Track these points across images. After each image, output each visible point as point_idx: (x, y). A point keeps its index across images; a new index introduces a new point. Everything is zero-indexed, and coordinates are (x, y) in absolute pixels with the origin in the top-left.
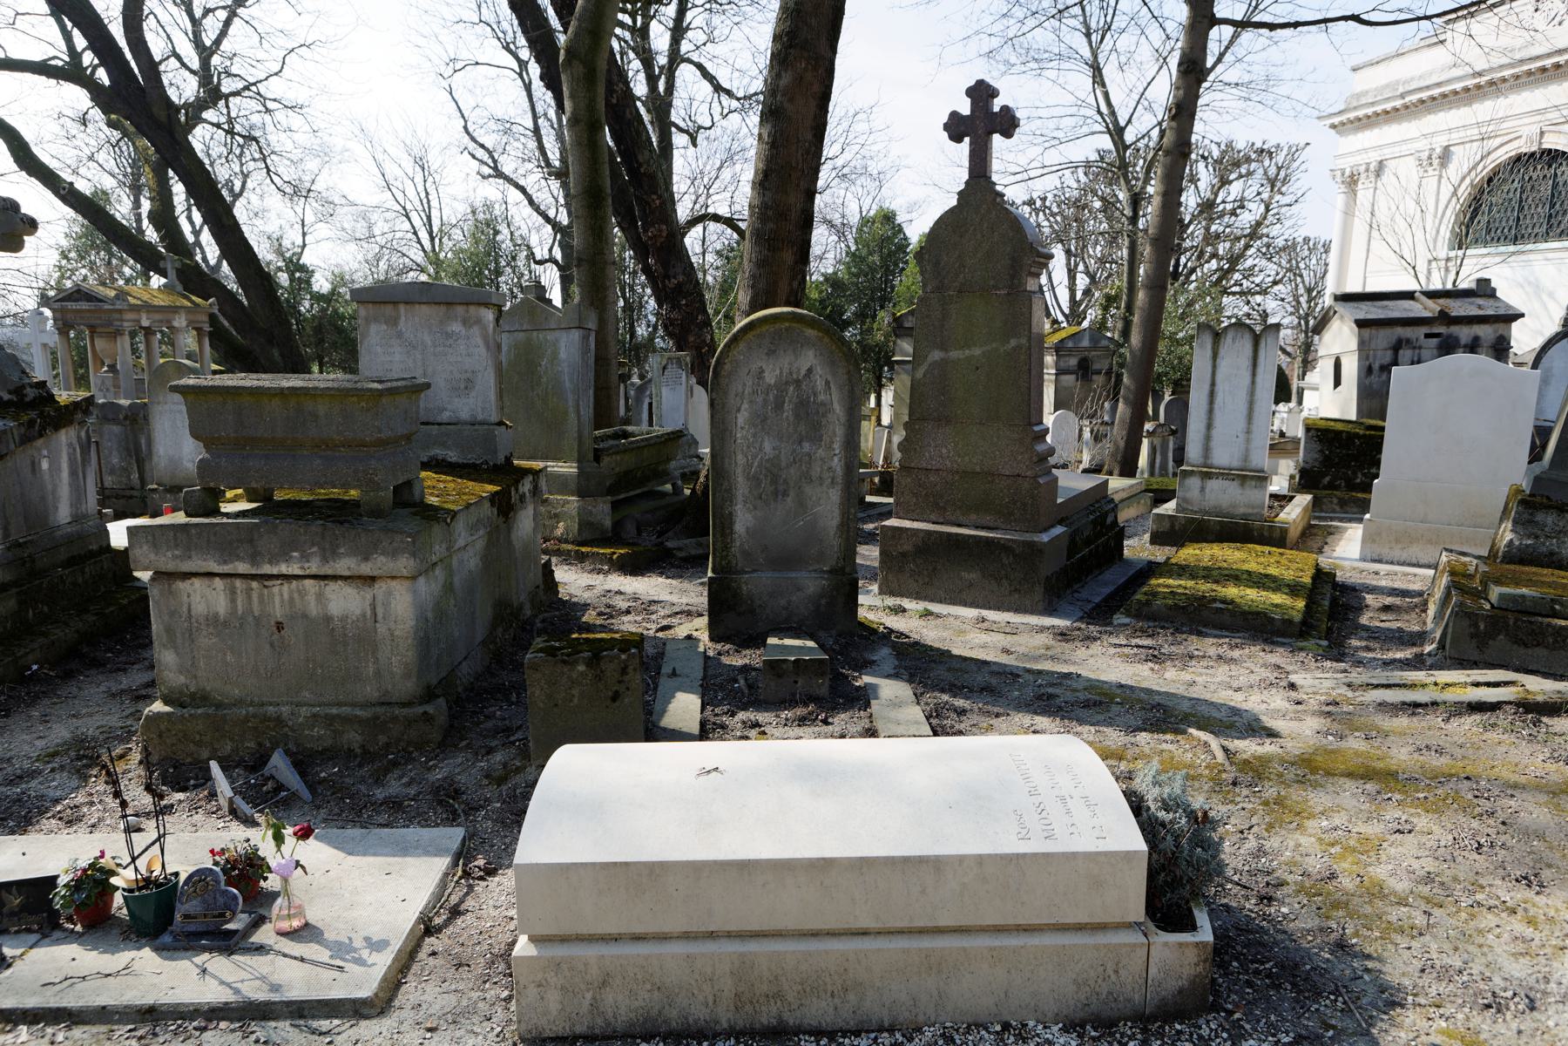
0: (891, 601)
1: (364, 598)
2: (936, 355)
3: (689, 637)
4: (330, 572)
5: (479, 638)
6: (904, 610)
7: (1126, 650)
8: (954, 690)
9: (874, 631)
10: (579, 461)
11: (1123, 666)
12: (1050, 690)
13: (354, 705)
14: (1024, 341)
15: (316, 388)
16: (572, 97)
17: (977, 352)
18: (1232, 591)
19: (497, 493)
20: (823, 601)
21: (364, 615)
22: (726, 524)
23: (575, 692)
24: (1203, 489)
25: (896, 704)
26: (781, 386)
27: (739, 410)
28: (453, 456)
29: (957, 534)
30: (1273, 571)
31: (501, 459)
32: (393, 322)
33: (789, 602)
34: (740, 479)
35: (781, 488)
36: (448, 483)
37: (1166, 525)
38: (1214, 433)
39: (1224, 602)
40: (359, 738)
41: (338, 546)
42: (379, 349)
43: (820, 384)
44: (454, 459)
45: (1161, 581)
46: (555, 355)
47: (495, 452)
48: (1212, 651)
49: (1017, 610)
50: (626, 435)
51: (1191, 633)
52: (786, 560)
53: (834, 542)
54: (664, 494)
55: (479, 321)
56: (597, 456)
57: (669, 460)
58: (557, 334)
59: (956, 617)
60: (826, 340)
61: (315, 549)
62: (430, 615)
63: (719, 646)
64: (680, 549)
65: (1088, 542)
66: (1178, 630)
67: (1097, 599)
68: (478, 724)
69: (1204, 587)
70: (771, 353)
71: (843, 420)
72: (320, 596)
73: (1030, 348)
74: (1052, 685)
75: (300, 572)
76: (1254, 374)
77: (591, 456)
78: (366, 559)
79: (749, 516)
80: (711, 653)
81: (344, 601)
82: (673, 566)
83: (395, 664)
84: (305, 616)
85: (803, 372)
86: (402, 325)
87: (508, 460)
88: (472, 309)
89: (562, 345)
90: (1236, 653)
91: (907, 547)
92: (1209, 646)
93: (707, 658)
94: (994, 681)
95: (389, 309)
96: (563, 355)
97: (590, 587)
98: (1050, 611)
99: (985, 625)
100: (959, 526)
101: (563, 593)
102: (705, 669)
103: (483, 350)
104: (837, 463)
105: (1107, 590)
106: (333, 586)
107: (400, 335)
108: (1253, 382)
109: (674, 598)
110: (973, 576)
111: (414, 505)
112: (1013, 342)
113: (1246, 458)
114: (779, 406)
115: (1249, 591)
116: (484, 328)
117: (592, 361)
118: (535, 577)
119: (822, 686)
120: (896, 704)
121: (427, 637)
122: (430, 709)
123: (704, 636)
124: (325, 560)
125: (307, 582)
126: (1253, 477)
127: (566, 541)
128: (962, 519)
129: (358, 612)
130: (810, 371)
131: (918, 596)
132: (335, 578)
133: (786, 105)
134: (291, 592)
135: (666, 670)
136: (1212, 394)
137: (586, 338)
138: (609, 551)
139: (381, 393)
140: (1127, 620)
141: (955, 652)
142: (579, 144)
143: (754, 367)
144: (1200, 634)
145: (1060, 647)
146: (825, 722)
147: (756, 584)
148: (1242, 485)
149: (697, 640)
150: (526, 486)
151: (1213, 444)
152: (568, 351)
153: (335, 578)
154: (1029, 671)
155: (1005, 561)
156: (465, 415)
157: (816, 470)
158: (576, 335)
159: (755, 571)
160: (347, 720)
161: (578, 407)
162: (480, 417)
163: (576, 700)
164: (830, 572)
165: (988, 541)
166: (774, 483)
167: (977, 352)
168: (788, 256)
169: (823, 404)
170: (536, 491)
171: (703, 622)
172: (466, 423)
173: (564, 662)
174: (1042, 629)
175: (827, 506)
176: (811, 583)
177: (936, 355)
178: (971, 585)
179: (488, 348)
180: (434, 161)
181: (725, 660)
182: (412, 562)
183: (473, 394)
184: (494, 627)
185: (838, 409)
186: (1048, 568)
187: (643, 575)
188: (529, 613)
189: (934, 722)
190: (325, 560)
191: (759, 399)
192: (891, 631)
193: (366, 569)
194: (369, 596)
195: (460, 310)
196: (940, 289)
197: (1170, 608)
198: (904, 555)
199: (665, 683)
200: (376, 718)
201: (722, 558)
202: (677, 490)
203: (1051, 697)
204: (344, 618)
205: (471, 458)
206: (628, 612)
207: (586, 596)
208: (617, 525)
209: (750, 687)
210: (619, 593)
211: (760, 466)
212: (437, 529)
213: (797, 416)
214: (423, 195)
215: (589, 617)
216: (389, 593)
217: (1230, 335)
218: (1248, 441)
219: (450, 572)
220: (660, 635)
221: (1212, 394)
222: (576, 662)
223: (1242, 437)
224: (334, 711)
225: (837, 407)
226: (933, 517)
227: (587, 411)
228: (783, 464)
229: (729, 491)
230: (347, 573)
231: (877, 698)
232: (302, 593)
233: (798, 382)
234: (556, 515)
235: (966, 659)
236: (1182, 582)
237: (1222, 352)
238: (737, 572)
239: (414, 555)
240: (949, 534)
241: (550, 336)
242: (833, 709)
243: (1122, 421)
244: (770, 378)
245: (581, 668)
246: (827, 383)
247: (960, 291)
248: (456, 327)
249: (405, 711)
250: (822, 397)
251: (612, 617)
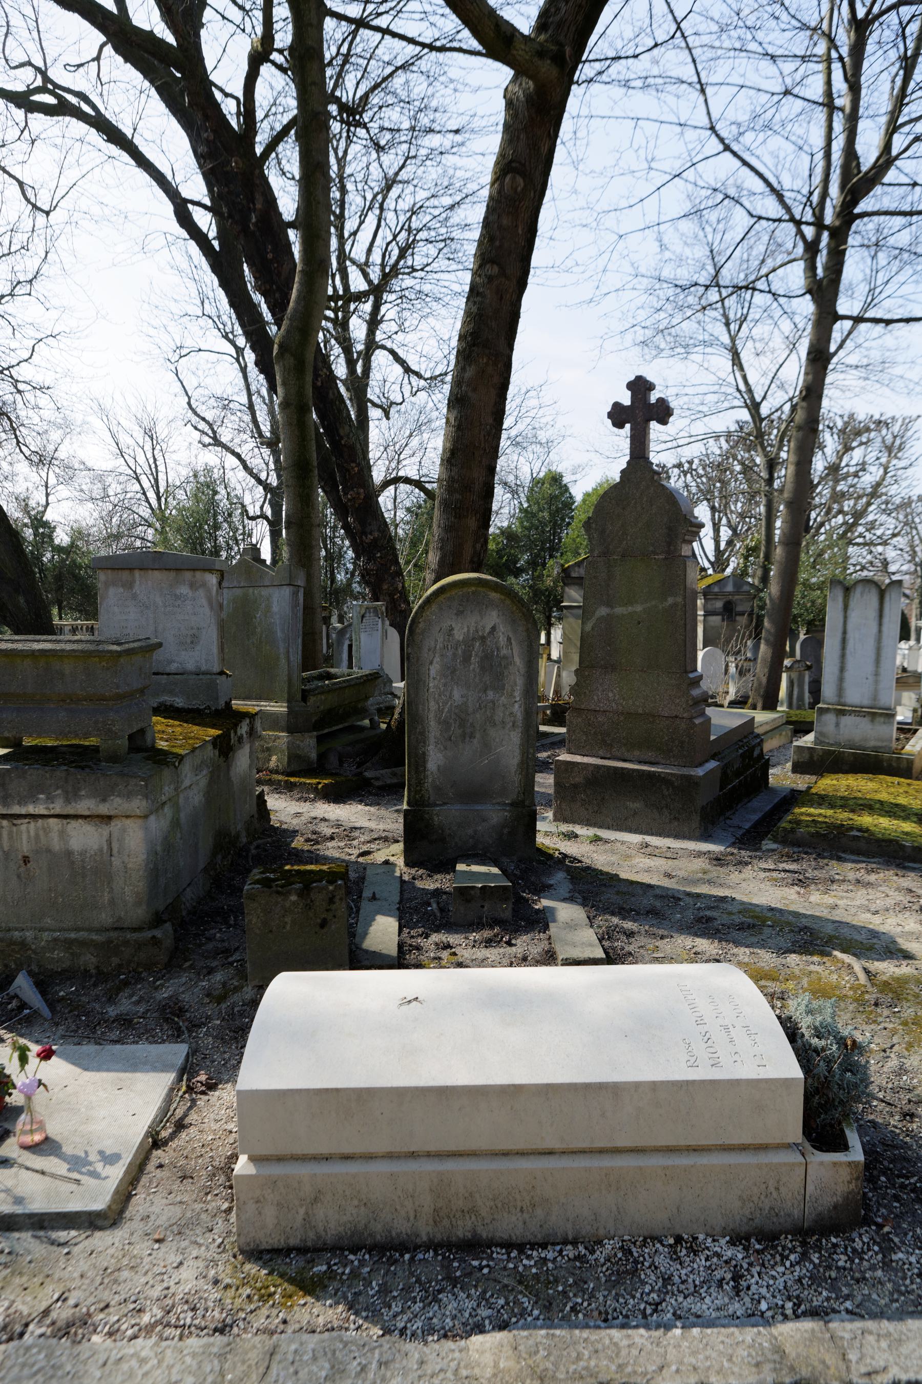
0: (565, 828)
1: (101, 835)
2: (603, 611)
3: (387, 862)
4: (72, 812)
5: (201, 866)
6: (576, 836)
7: (775, 874)
8: (623, 913)
9: (550, 857)
10: (289, 701)
11: (772, 890)
12: (708, 913)
13: (90, 930)
14: (679, 599)
15: (63, 650)
16: (284, 384)
17: (639, 608)
18: (866, 820)
19: (218, 736)
20: (506, 831)
21: (101, 850)
22: (419, 763)
23: (288, 919)
24: (837, 725)
25: (571, 926)
26: (468, 643)
27: (431, 663)
28: (180, 702)
29: (623, 769)
30: (902, 801)
31: (222, 704)
32: (129, 585)
34: (432, 723)
35: (468, 731)
36: (176, 728)
37: (806, 756)
38: (848, 675)
39: (860, 830)
40: (94, 960)
41: (79, 789)
42: (116, 609)
43: (502, 640)
44: (180, 705)
45: (803, 810)
46: (269, 607)
47: (217, 699)
48: (851, 876)
49: (677, 836)
50: (329, 676)
51: (831, 859)
52: (473, 794)
54: (363, 729)
55: (204, 585)
56: (305, 695)
57: (367, 698)
58: (271, 590)
59: (623, 843)
60: (508, 602)
61: (59, 792)
62: (159, 848)
63: (413, 871)
64: (377, 779)
65: (738, 774)
66: (820, 856)
67: (747, 826)
68: (200, 945)
69: (843, 816)
70: (459, 613)
71: (523, 671)
72: (62, 833)
73: (685, 606)
74: (710, 908)
75: (45, 812)
76: (880, 624)
77: (299, 696)
78: (104, 800)
79: (440, 755)
80: (406, 878)
81: (83, 838)
82: (370, 794)
83: (128, 891)
84: (49, 851)
85: (488, 630)
86: (137, 588)
87: (228, 704)
88: (198, 574)
89: (275, 599)
90: (872, 878)
91: (579, 779)
92: (848, 870)
93: (403, 882)
94: (658, 904)
95: (125, 575)
96: (275, 608)
97: (298, 815)
98: (706, 837)
99: (649, 849)
100: (625, 760)
101: (274, 821)
102: (402, 892)
103: (207, 610)
104: (518, 709)
105: (755, 817)
106: (74, 824)
107: (134, 597)
108: (880, 631)
109: (372, 825)
110: (636, 805)
111: (146, 750)
112: (670, 600)
113: (875, 697)
114: (466, 659)
115: (882, 820)
116: (209, 591)
117: (300, 614)
118: (250, 807)
119: (505, 910)
120: (571, 926)
121: (157, 869)
122: (158, 933)
123: (400, 861)
124: (68, 801)
125: (51, 820)
126: (881, 714)
127: (277, 772)
128: (627, 755)
129: (96, 847)
130: (494, 629)
131: (589, 823)
132: (76, 817)
133: (470, 394)
134: (37, 830)
135: (367, 894)
136: (844, 641)
137: (295, 594)
138: (315, 781)
139: (119, 654)
140: (774, 846)
141: (623, 876)
142: (290, 424)
143: (445, 625)
144: (839, 859)
145: (716, 872)
146: (509, 944)
147: (447, 815)
148: (872, 721)
149: (394, 865)
150: (243, 729)
151: (847, 684)
152: (279, 604)
153: (76, 817)
154: (689, 894)
155: (666, 792)
156: (190, 666)
157: (499, 715)
158: (287, 591)
159: (445, 804)
160: (83, 943)
161: (287, 653)
162: (204, 668)
163: (288, 927)
164: (511, 805)
165: (650, 775)
166: (461, 727)
167: (639, 608)
168: (472, 523)
169: (505, 657)
170: (252, 732)
171: (399, 847)
172: (191, 673)
173: (278, 893)
174: (700, 854)
175: (508, 747)
176: (495, 815)
177: (603, 611)
178: (635, 813)
179: (212, 608)
180: (161, 431)
181: (419, 884)
182: (144, 803)
183: (198, 648)
184: (214, 854)
185: (518, 661)
186: (704, 798)
187: (344, 802)
188: (244, 840)
189: (606, 944)
190: (68, 801)
191: (450, 654)
192: (565, 856)
193: (104, 809)
194: (106, 833)
195: (188, 575)
196: (605, 554)
197: (812, 835)
198: (575, 786)
199: (366, 906)
200: (110, 941)
202: (374, 725)
203: (709, 919)
204: (83, 853)
205: (195, 704)
206: (332, 838)
207: (295, 823)
208: (322, 756)
209: (441, 910)
210: (324, 820)
211: (450, 711)
212: (167, 773)
213: (483, 668)
214: (151, 461)
215: (298, 843)
216: (124, 830)
217: (859, 589)
218: (876, 682)
219: (177, 809)
220: (361, 860)
221: (844, 641)
222: (289, 893)
223: (871, 678)
224: (73, 935)
225: (517, 660)
226: (601, 753)
227: (296, 657)
228: (470, 710)
229: (422, 733)
230: (87, 813)
231: (554, 921)
232: (47, 831)
233: (483, 639)
234: (268, 749)
235: (632, 883)
236: (822, 811)
237: (853, 604)
238: (429, 805)
239: (146, 797)
240: (616, 768)
241: (265, 592)
242: (516, 931)
243: (764, 660)
244: (459, 635)
245: (294, 898)
246: (509, 639)
247: (623, 556)
248: (184, 590)
249: (136, 935)
250: (504, 652)
251: (317, 843)
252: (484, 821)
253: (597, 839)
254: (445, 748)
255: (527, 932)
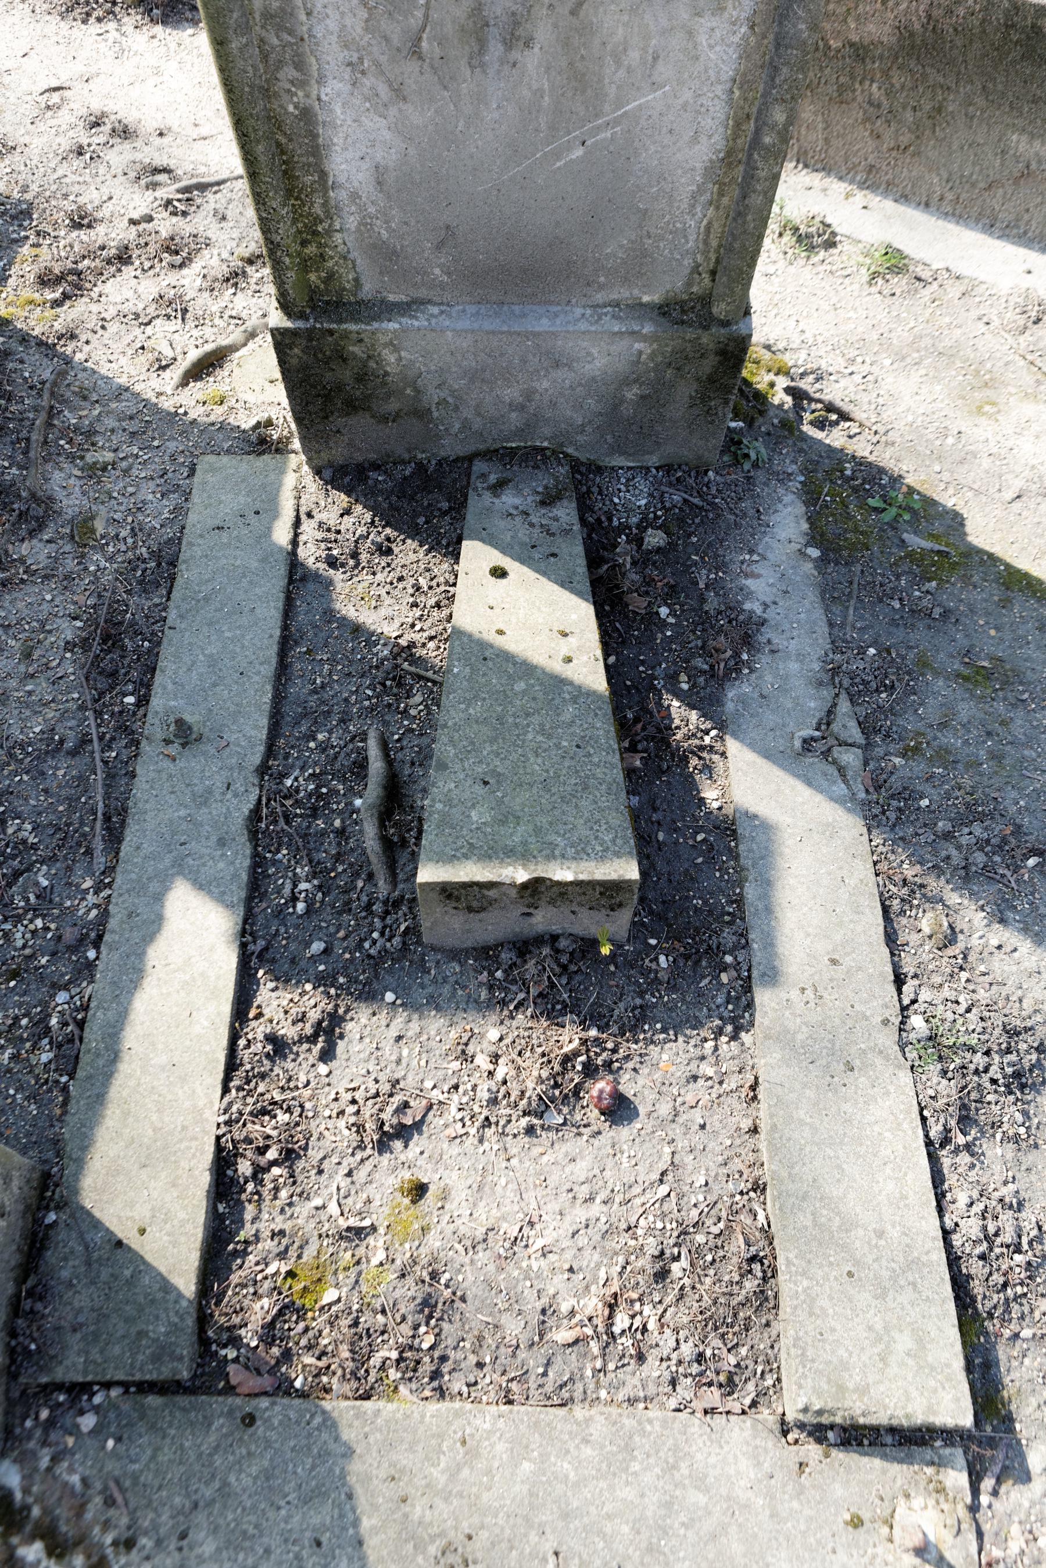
20: (631, 394)
33: (529, 395)
52: (520, 274)
53: (686, 222)
79: (377, 125)
93: (296, 575)
102: (283, 669)
146: (619, 1109)
147: (427, 347)
178: (1026, 174)
198: (860, 52)
201: (305, 265)
231: (772, 976)
252: (557, 365)
253: (894, 263)
254: (399, 93)
255: (675, 1027)
